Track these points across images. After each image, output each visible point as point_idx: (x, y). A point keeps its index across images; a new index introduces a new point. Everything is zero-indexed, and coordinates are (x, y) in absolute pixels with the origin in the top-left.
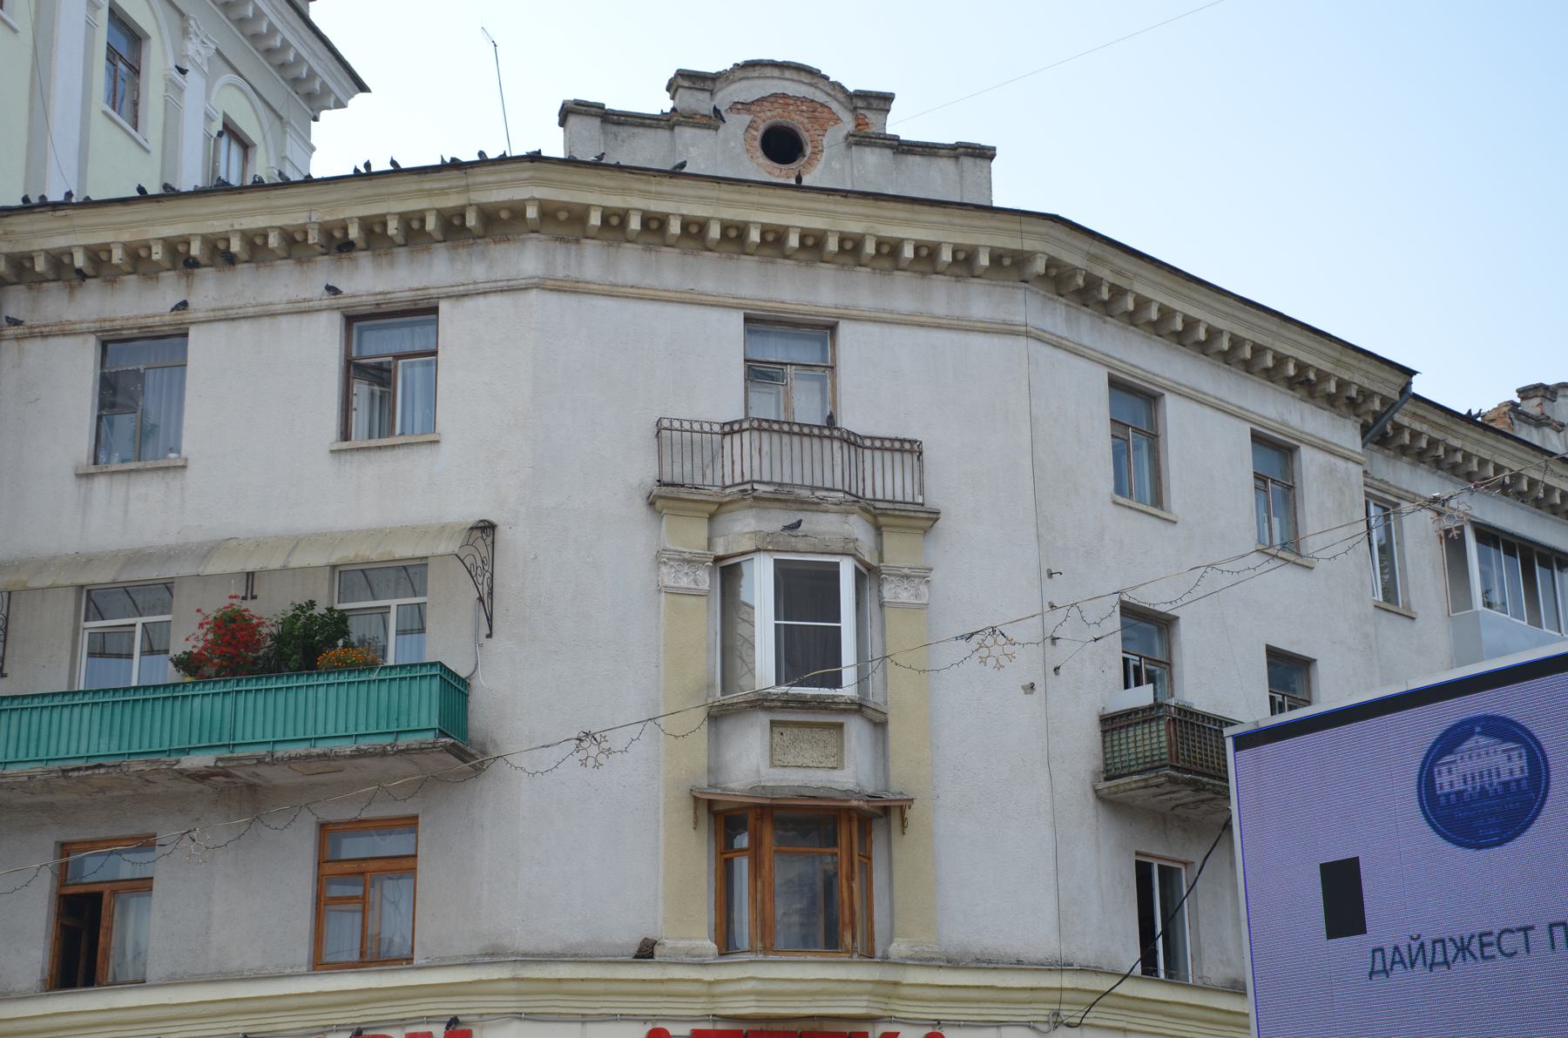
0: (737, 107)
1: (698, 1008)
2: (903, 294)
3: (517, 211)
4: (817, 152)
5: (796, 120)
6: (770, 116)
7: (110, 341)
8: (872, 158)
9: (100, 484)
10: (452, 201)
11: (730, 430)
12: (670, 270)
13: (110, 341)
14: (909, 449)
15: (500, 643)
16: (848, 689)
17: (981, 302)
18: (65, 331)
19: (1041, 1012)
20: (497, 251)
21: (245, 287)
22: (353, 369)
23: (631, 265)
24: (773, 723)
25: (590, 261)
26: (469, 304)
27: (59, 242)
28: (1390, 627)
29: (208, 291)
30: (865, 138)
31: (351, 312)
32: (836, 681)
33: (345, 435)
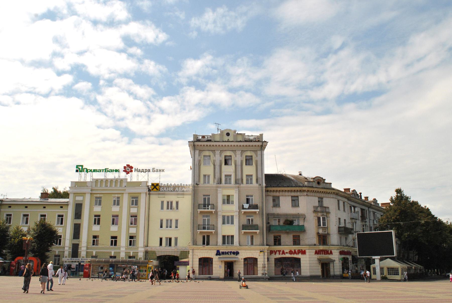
0: (316, 180)
1: (318, 249)
2: (327, 195)
3: (305, 190)
4: (321, 184)
5: (319, 181)
6: (318, 181)
7: (273, 197)
8: (324, 184)
9: (274, 208)
10: (301, 189)
11: (318, 207)
12: (314, 194)
13: (273, 197)
14: (328, 208)
15: (305, 222)
16: (326, 226)
17: (332, 196)
18: (270, 196)
19: (337, 249)
20: (303, 193)
21: (284, 193)
22: (292, 200)
23: (311, 194)
24: (323, 229)
25: (309, 194)
26: (301, 197)
27: (271, 189)
28: (338, 211)
29: (281, 193)
30: (324, 183)
31: (292, 196)
32: (326, 226)
33: (292, 206)
